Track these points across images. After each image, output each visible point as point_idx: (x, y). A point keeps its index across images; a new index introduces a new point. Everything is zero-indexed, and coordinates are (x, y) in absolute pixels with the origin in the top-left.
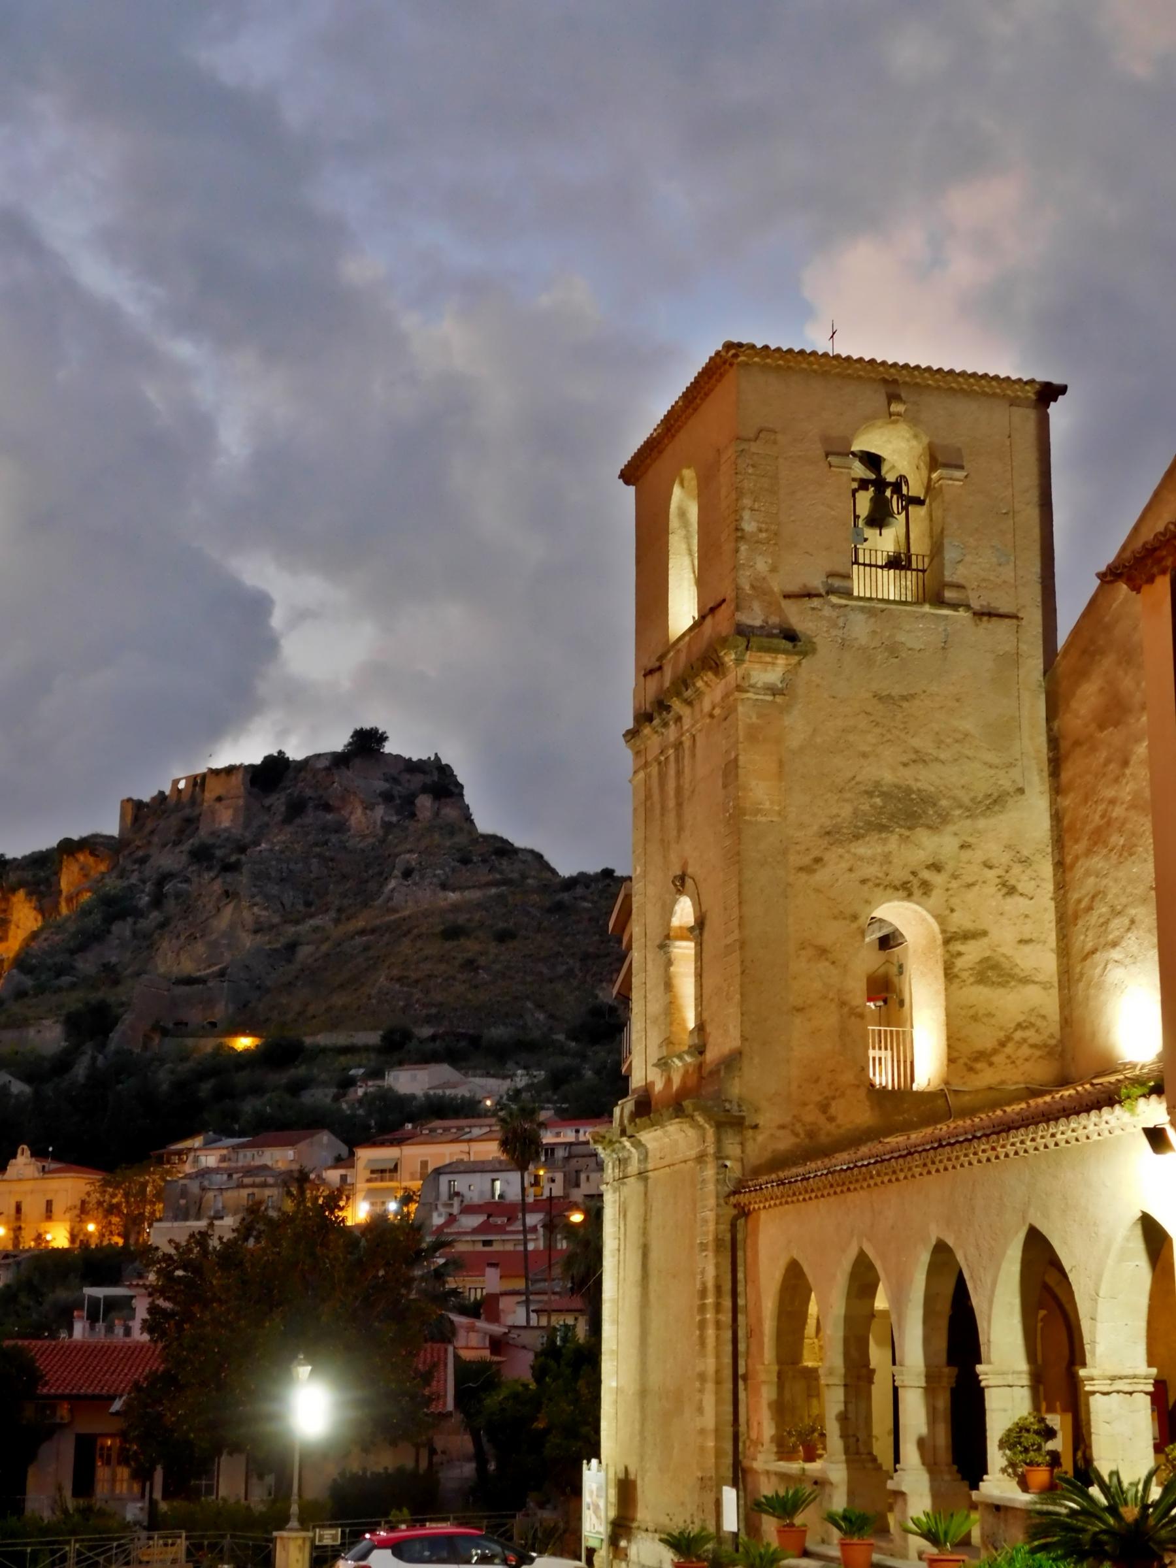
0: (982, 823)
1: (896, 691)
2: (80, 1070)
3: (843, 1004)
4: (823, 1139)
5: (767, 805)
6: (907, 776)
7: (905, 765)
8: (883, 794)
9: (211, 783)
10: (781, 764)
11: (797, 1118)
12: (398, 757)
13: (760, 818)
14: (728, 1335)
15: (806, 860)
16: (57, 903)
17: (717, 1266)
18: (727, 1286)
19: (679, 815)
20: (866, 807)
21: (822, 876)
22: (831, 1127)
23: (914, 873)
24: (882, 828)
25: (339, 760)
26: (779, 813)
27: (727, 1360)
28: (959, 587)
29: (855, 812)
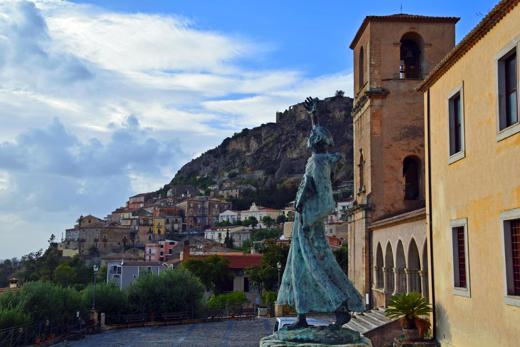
2: (268, 184)
3: (397, 180)
4: (392, 212)
5: (378, 132)
7: (414, 120)
8: (409, 128)
9: (299, 107)
10: (381, 122)
11: (385, 208)
12: (348, 97)
13: (376, 136)
14: (368, 259)
16: (261, 140)
17: (365, 243)
18: (368, 248)
20: (403, 132)
22: (394, 210)
23: (416, 148)
24: (407, 137)
25: (333, 99)
26: (381, 134)
27: (368, 265)
29: (400, 134)
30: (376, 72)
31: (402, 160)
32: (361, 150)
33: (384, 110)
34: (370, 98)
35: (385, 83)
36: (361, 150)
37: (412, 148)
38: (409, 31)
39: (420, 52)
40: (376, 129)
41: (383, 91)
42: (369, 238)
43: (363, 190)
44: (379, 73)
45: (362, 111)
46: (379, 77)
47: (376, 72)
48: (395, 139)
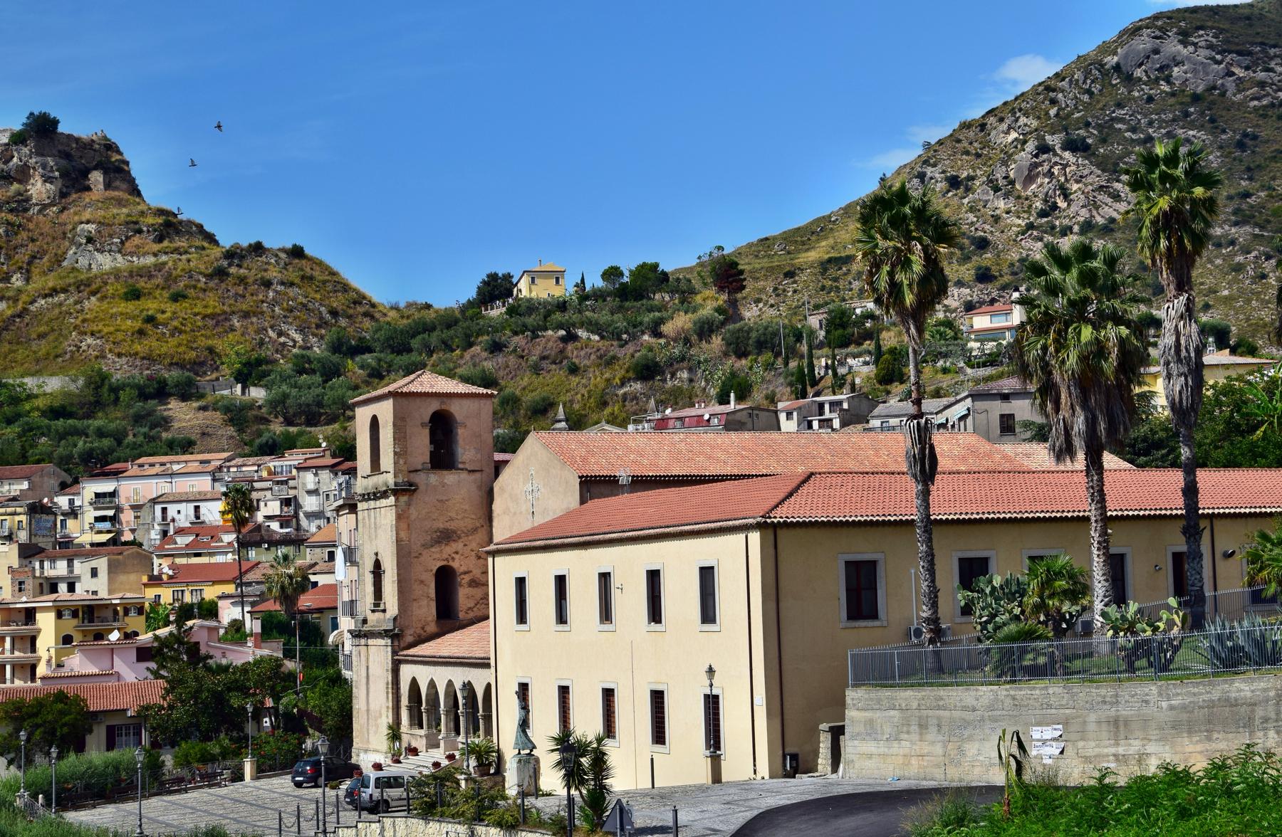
6: (448, 525)
21: (422, 559)
30: (401, 462)
31: (435, 569)
37: (445, 556)
41: (411, 485)
42: (396, 672)
46: (405, 468)
47: (401, 462)
48: (425, 546)
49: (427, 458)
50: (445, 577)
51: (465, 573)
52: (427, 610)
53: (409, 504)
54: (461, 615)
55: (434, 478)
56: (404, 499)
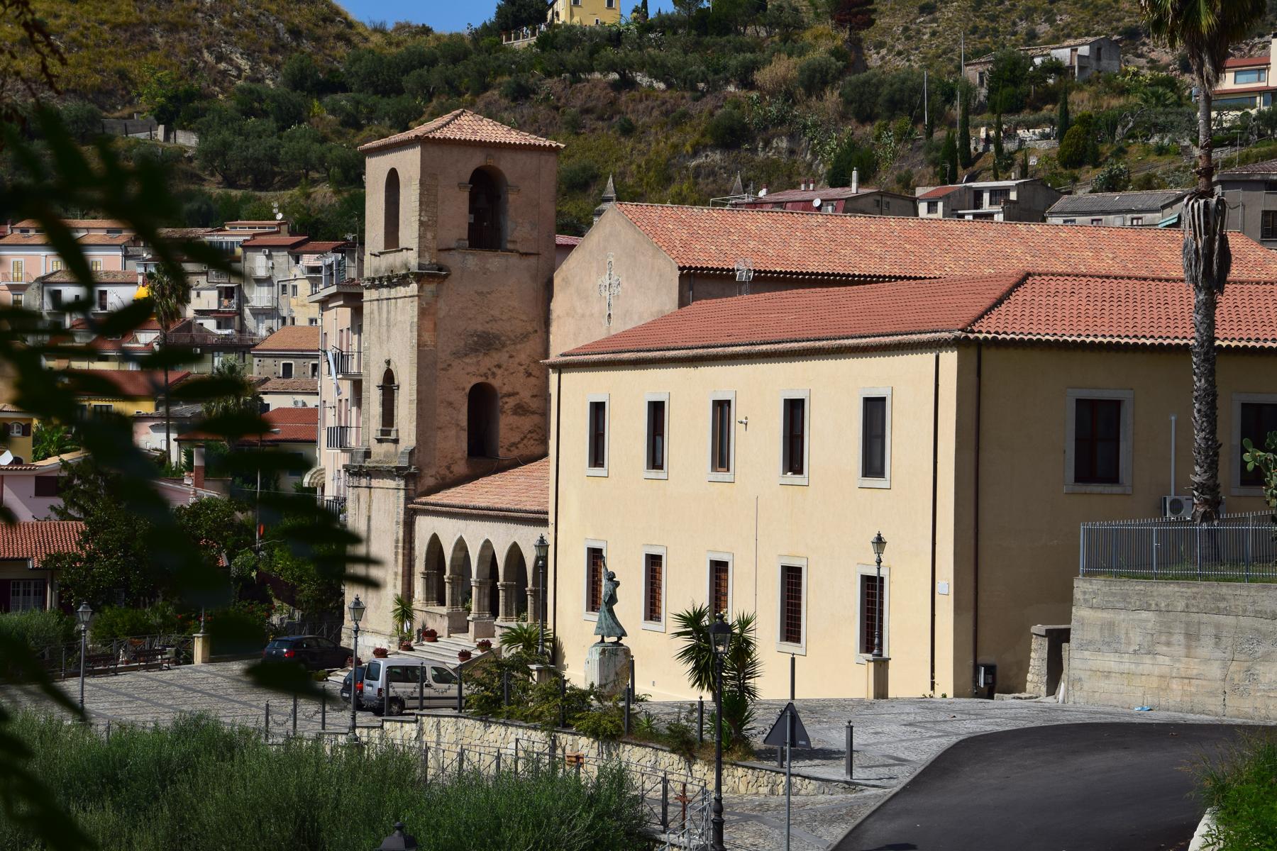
0: (518, 347)
1: (485, 290)
15: (444, 366)
19: (388, 331)
24: (477, 351)
28: (514, 242)
30: (429, 236)
31: (467, 390)
32: (388, 362)
33: (442, 304)
34: (417, 282)
35: (443, 254)
36: (388, 362)
37: (483, 370)
38: (483, 163)
39: (499, 197)
40: (427, 337)
43: (393, 436)
44: (434, 238)
45: (394, 292)
46: (433, 245)
47: (429, 236)
48: (457, 355)
49: (464, 233)
50: (482, 401)
51: (510, 395)
52: (455, 443)
53: (436, 296)
54: (502, 453)
55: (472, 261)
56: (430, 287)
